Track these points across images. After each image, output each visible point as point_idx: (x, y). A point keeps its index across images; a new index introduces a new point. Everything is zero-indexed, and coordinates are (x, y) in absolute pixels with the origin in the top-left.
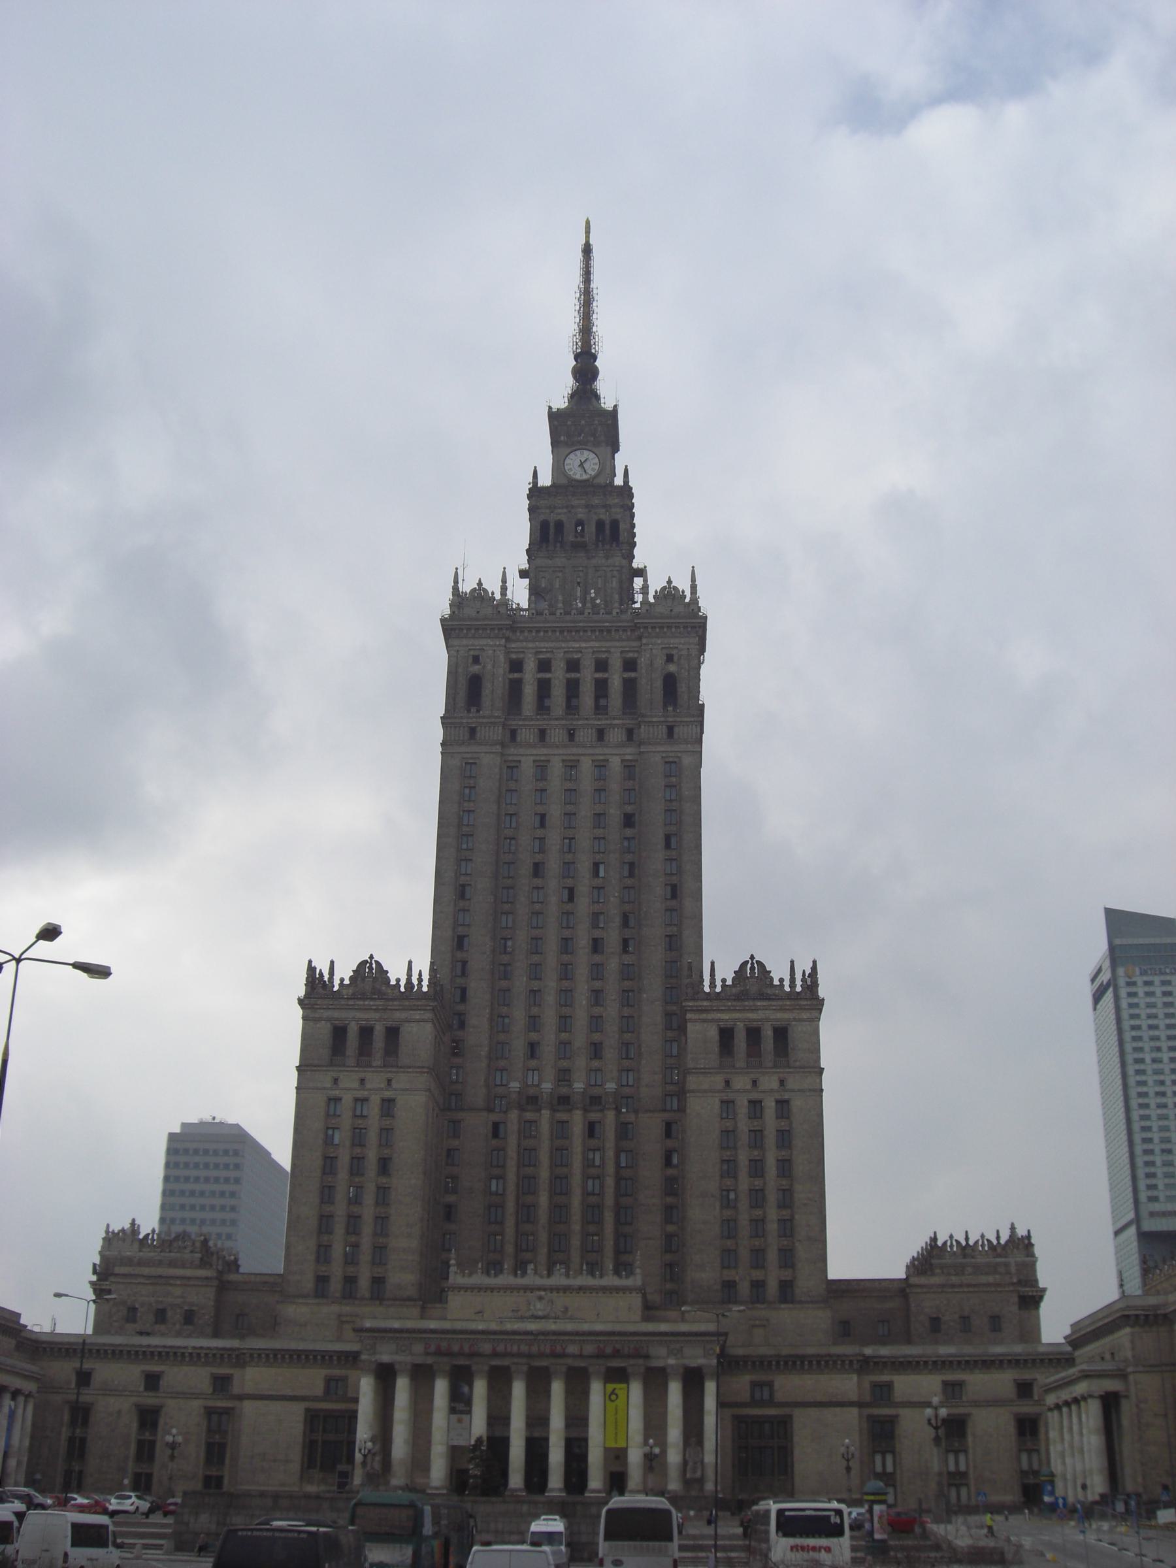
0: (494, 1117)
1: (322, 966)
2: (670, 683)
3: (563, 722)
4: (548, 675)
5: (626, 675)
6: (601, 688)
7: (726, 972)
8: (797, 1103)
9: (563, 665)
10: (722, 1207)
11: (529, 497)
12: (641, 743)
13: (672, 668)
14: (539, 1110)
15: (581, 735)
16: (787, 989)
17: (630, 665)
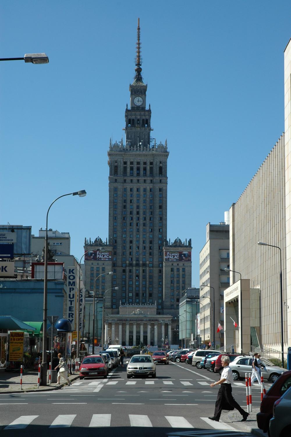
0: (123, 268)
1: (88, 239)
2: (161, 169)
3: (136, 178)
4: (132, 166)
5: (151, 166)
6: (145, 169)
7: (172, 241)
8: (186, 269)
9: (136, 163)
10: (171, 290)
11: (126, 112)
12: (154, 183)
13: (161, 165)
14: (133, 267)
15: (140, 181)
16: (185, 245)
17: (151, 163)
